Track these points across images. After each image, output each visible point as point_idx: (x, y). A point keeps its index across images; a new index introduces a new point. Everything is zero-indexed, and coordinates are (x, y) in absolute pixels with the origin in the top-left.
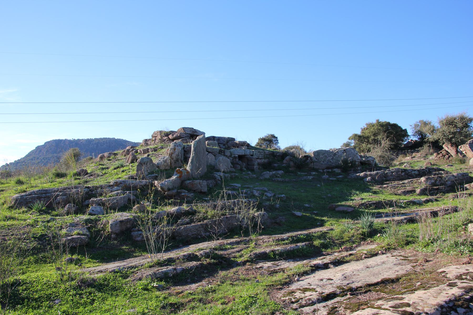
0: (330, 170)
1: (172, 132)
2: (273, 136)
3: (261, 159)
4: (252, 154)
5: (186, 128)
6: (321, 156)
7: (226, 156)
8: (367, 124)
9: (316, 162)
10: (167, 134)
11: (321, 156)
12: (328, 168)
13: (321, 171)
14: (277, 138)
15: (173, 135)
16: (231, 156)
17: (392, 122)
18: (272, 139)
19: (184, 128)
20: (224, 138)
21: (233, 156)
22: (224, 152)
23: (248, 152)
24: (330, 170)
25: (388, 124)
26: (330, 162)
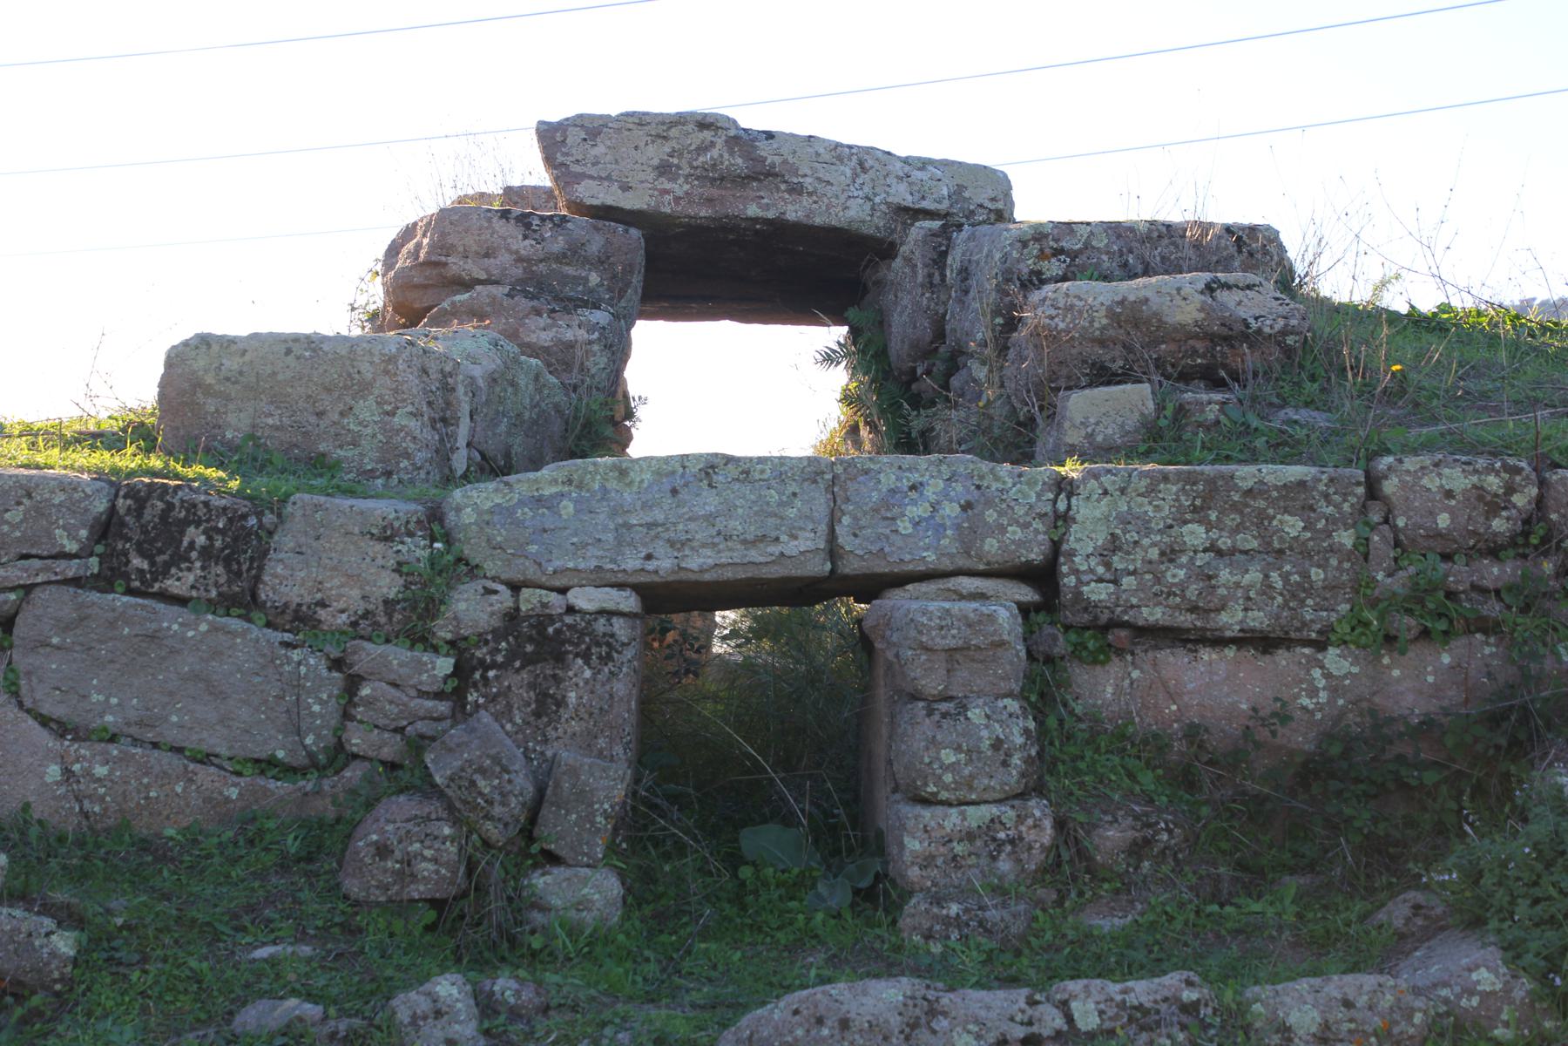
3: (1263, 642)
5: (592, 128)
7: (300, 621)
21: (471, 609)
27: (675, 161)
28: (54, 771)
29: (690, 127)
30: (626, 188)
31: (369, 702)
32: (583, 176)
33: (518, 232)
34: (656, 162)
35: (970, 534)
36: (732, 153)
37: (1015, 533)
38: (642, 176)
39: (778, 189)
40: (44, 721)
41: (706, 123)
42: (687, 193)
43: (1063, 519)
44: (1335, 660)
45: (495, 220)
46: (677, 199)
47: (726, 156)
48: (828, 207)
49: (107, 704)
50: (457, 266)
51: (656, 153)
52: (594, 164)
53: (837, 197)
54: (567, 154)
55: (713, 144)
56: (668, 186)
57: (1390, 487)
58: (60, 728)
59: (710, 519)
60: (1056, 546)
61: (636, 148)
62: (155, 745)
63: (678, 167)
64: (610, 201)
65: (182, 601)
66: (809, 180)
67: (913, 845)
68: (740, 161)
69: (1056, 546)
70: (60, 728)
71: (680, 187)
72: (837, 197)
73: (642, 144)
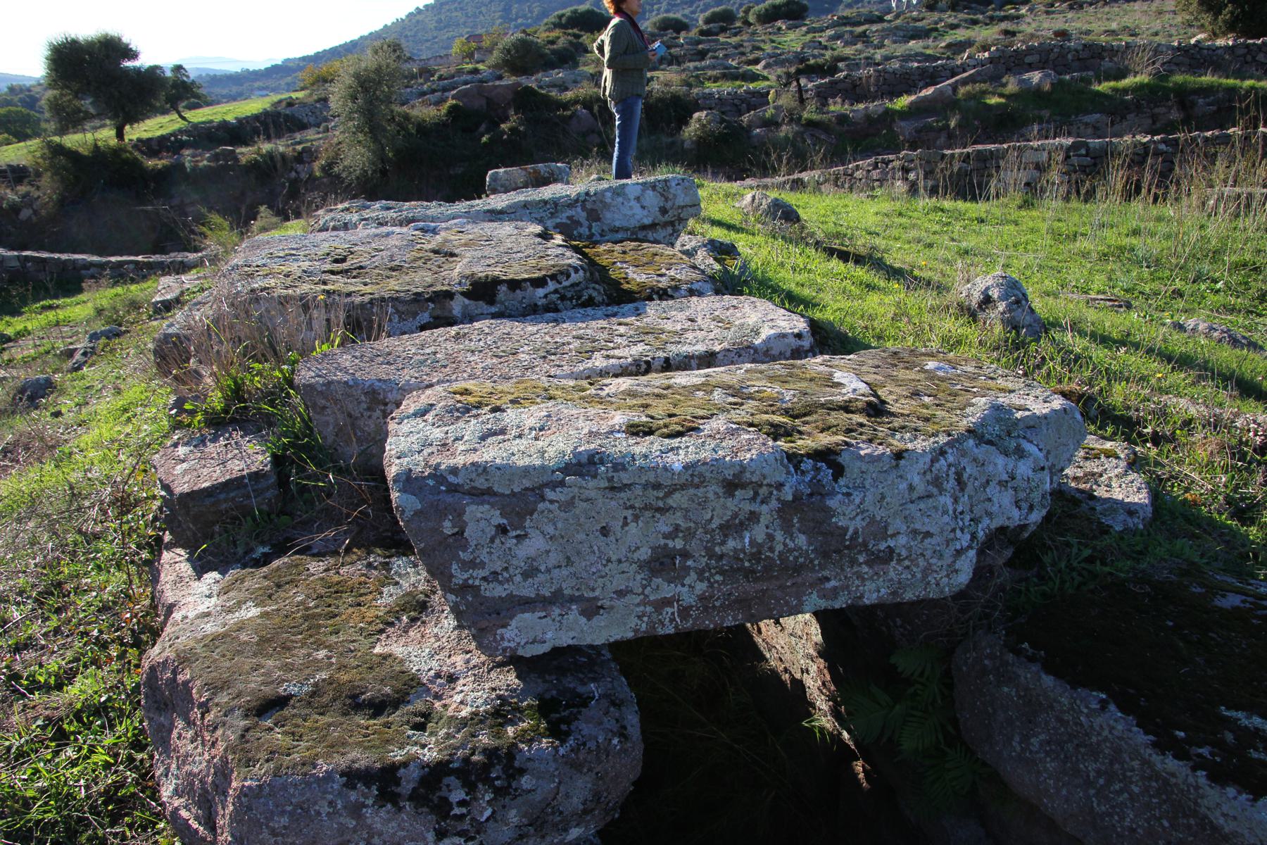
27: (678, 544)
29: (713, 489)
30: (592, 609)
34: (644, 553)
36: (787, 528)
38: (619, 583)
39: (853, 562)
42: (702, 598)
45: (368, 812)
46: (685, 612)
47: (779, 536)
48: (927, 571)
51: (640, 538)
52: (526, 575)
53: (941, 557)
54: (473, 564)
55: (754, 517)
56: (668, 590)
61: (605, 531)
63: (685, 555)
64: (565, 640)
66: (902, 540)
68: (802, 540)
71: (690, 590)
72: (941, 557)
73: (616, 526)
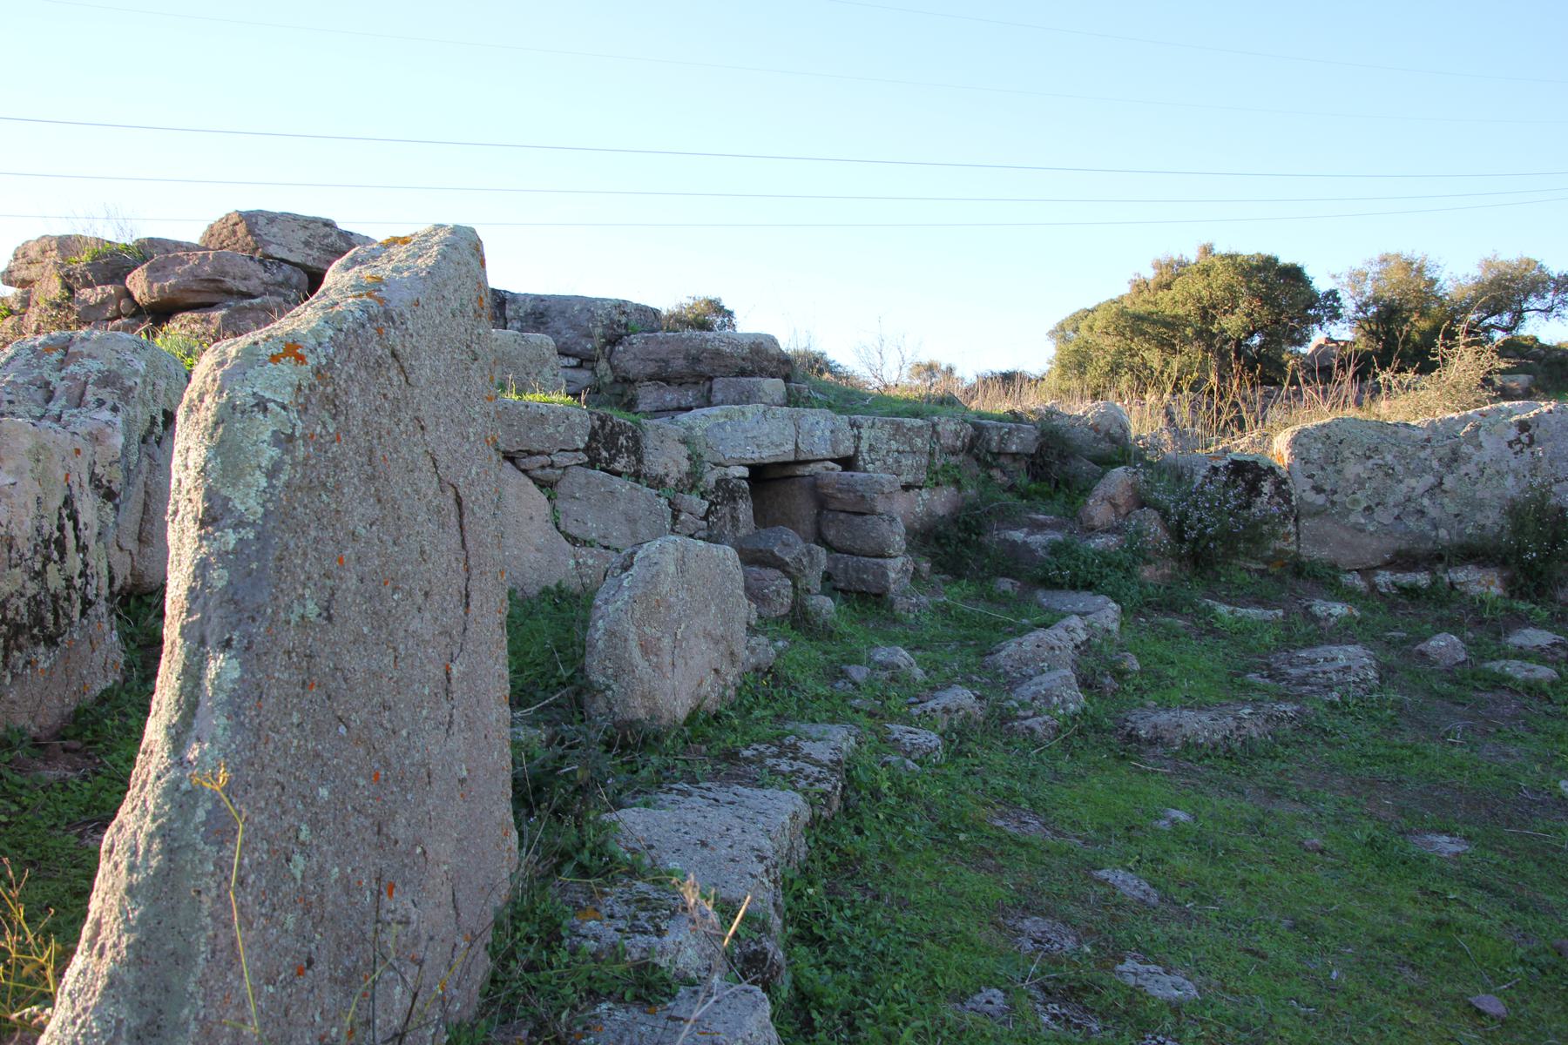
0: (1422, 579)
1: (151, 252)
2: (716, 307)
4: (846, 448)
5: (272, 218)
6: (1353, 469)
7: (658, 483)
8: (1158, 265)
9: (1318, 512)
10: (113, 265)
11: (1353, 469)
12: (1403, 560)
13: (1360, 583)
14: (730, 314)
15: (156, 271)
16: (692, 481)
17: (1285, 259)
18: (709, 318)
19: (251, 220)
20: (588, 304)
21: (711, 478)
22: (636, 450)
23: (820, 433)
24: (1422, 579)
25: (1269, 263)
26: (1421, 513)
28: (572, 562)
30: (291, 251)
31: (682, 523)
32: (270, 243)
33: (261, 268)
35: (835, 443)
37: (847, 443)
40: (568, 537)
41: (328, 224)
43: (858, 438)
44: (925, 494)
49: (592, 528)
50: (230, 283)
51: (302, 235)
57: (939, 428)
58: (573, 540)
59: (767, 435)
60: (857, 448)
62: (607, 548)
65: (619, 474)
67: (892, 575)
69: (857, 448)
70: (573, 540)
71: (316, 254)
